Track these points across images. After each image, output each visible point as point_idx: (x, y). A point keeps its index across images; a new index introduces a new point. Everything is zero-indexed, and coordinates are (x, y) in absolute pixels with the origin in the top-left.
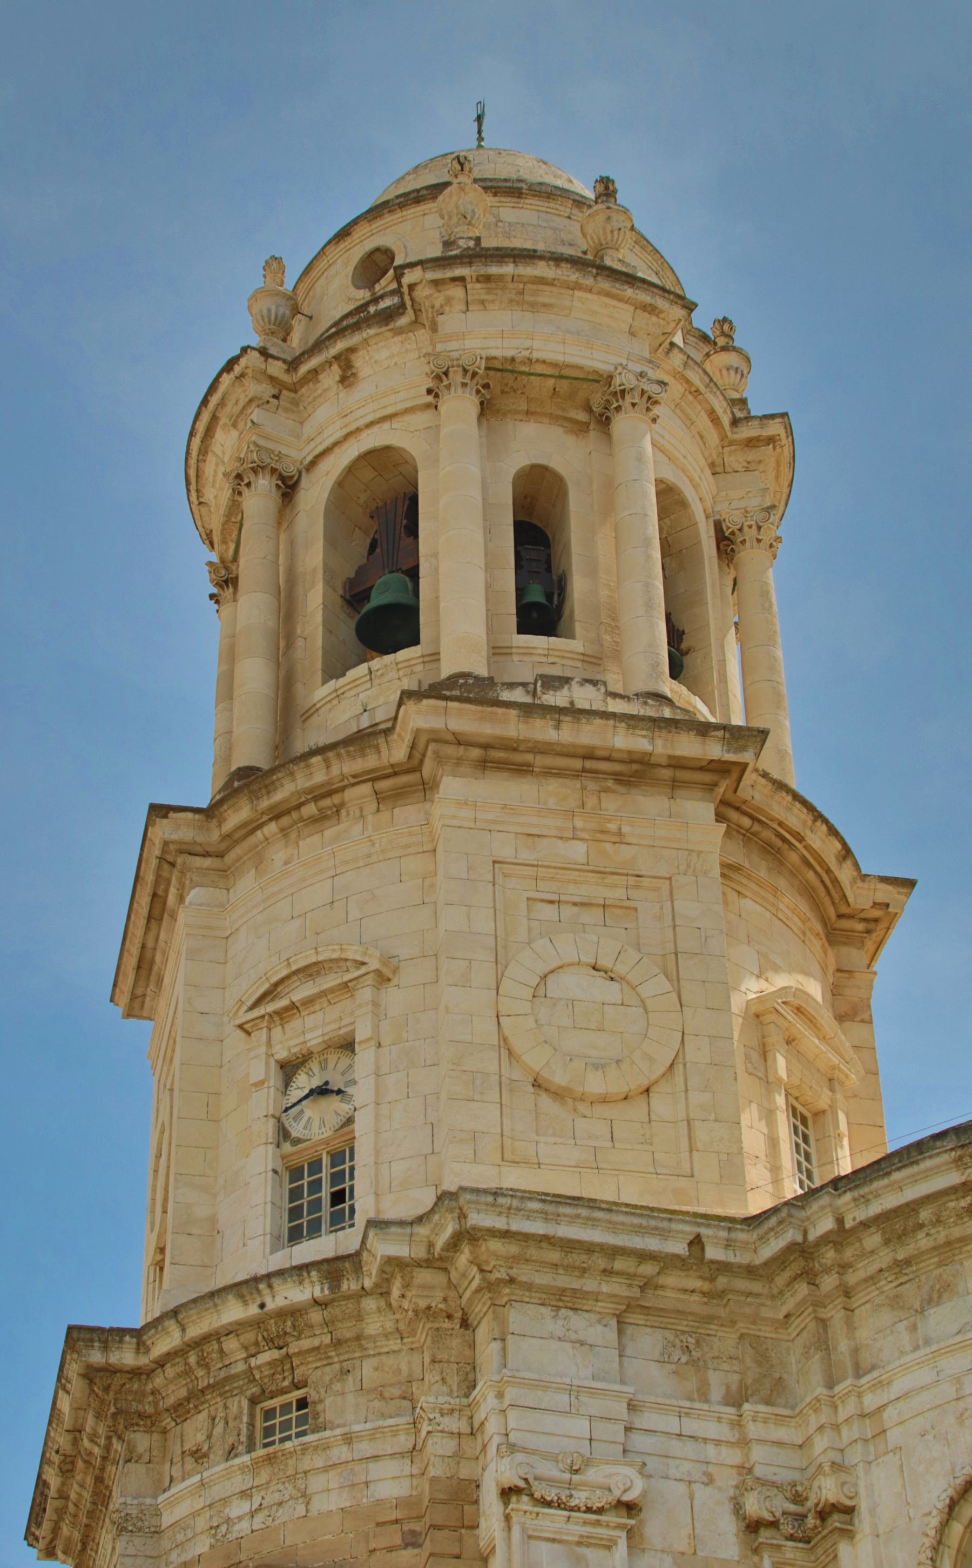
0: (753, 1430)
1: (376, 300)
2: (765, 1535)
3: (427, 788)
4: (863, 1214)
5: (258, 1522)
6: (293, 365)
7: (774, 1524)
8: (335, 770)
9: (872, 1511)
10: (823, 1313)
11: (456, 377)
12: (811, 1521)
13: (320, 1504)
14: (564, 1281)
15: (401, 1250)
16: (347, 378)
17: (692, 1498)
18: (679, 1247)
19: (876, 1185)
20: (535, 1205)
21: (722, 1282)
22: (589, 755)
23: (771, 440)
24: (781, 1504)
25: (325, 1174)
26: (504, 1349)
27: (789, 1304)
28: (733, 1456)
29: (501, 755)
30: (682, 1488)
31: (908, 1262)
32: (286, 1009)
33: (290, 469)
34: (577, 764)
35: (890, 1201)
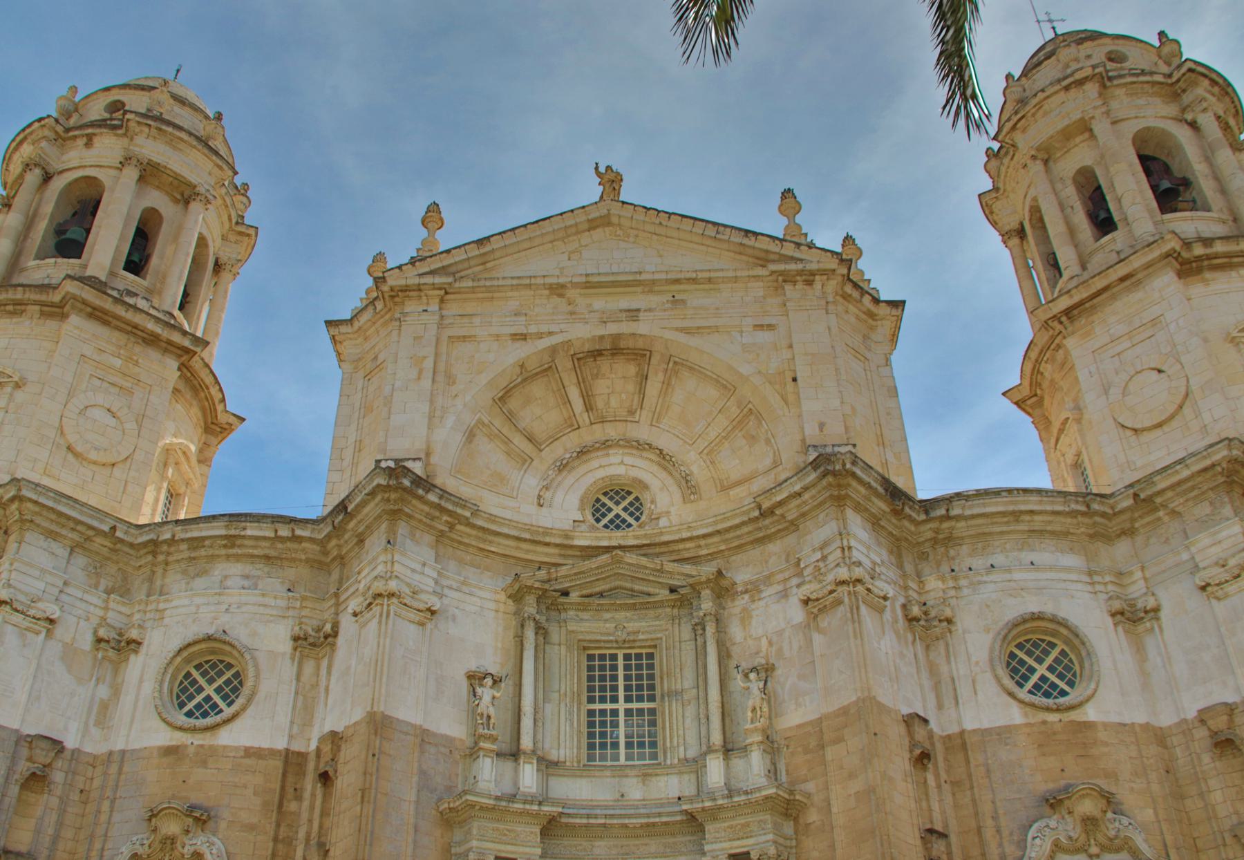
0: (112, 605)
1: (111, 119)
2: (103, 645)
3: (64, 317)
6: (68, 130)
7: (108, 642)
8: (27, 296)
10: (155, 569)
11: (134, 162)
14: (54, 527)
16: (89, 144)
17: (78, 624)
18: (106, 528)
20: (52, 494)
21: (119, 546)
22: (136, 327)
23: (249, 235)
24: (113, 635)
26: (19, 547)
27: (143, 562)
28: (101, 613)
29: (100, 314)
30: (75, 619)
31: (194, 558)
33: (51, 171)
34: (130, 329)
35: (196, 534)
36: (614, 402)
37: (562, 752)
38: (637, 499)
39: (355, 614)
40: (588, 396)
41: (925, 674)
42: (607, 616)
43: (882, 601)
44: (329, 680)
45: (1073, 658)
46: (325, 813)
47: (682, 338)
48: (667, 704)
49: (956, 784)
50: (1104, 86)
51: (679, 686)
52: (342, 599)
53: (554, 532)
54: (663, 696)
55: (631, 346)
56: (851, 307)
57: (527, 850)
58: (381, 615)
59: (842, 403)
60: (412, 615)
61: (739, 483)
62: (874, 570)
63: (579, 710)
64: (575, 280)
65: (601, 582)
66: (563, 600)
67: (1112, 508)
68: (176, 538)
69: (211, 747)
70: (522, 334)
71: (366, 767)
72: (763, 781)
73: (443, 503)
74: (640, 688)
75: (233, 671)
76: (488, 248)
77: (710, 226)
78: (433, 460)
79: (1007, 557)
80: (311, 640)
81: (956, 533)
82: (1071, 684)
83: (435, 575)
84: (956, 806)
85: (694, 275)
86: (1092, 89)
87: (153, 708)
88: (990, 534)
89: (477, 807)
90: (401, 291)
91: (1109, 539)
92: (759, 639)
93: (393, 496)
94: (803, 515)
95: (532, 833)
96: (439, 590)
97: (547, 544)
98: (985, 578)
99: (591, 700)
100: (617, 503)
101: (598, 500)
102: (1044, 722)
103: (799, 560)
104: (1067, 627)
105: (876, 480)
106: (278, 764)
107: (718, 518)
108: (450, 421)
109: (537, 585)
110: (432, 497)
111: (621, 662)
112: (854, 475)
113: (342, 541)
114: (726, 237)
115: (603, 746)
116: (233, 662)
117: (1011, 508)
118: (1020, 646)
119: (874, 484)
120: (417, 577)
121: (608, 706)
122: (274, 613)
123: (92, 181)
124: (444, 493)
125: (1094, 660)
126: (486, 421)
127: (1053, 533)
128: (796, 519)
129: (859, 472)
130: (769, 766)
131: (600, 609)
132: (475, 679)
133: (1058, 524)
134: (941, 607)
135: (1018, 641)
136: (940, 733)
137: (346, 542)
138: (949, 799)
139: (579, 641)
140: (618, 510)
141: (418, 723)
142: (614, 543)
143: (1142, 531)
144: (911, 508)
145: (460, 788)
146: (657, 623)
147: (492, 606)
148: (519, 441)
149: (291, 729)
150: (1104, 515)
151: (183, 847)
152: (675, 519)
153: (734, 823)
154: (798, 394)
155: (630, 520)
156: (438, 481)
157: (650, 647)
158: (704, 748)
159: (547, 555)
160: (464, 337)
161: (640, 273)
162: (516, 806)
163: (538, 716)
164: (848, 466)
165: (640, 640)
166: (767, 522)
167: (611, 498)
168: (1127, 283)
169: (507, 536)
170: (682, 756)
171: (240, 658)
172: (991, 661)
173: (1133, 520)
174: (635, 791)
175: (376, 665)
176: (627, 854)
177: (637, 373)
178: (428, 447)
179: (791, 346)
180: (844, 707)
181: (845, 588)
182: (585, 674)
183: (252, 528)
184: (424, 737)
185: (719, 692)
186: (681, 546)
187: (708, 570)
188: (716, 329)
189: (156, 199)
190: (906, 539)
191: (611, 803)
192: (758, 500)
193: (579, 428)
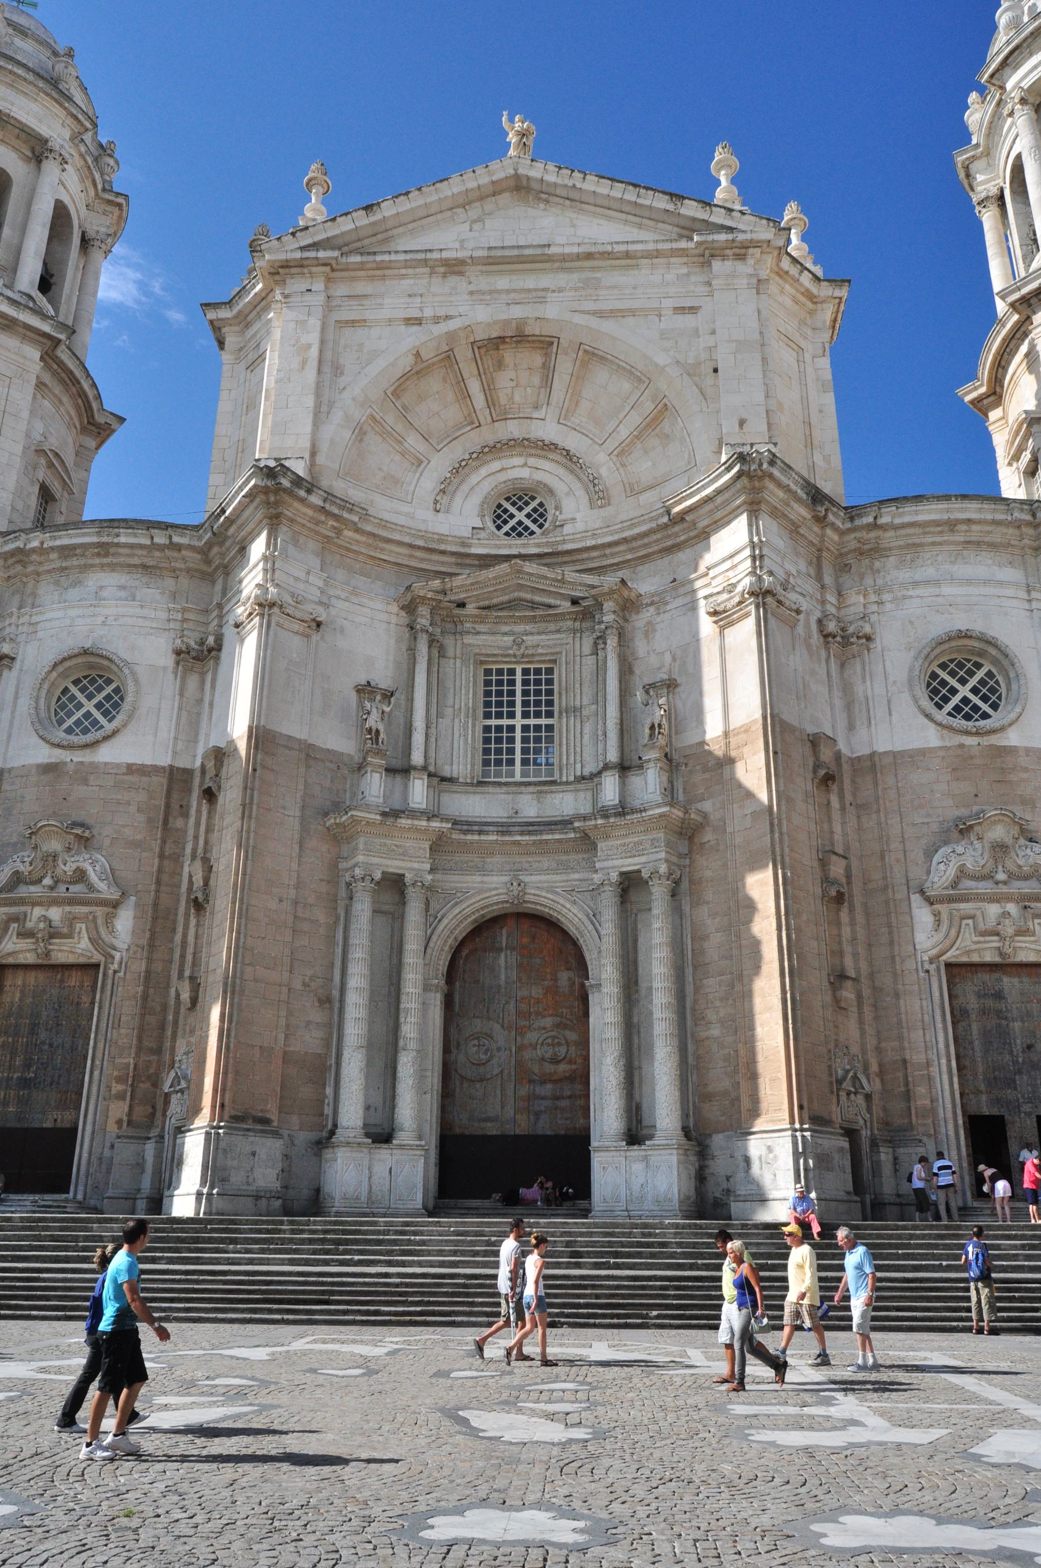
4: (51, 544)
9: (22, 661)
10: (25, 579)
23: (119, 205)
27: (12, 572)
36: (517, 398)
38: (541, 505)
41: (837, 693)
42: (506, 628)
47: (594, 322)
51: (578, 703)
54: (560, 713)
55: (537, 333)
56: (787, 287)
57: (416, 866)
58: (261, 626)
59: (767, 397)
60: (296, 626)
62: (787, 581)
63: (474, 726)
64: (477, 254)
66: (458, 611)
69: (91, 764)
72: (658, 798)
73: (327, 506)
74: (537, 703)
75: (113, 686)
78: (320, 459)
80: (193, 654)
81: (884, 544)
82: (995, 706)
83: (321, 584)
84: (860, 829)
85: (609, 248)
88: (921, 545)
90: (282, 267)
96: (325, 600)
97: (443, 552)
98: (910, 593)
99: (487, 715)
100: (520, 509)
101: (499, 506)
102: (961, 746)
104: (996, 646)
105: (796, 483)
106: (165, 781)
108: (337, 416)
110: (315, 499)
111: (519, 677)
112: (771, 476)
114: (647, 202)
115: (498, 763)
117: (945, 517)
118: (943, 666)
119: (793, 487)
120: (301, 586)
121: (505, 722)
122: (154, 625)
124: (329, 496)
129: (776, 472)
130: (666, 785)
131: (498, 621)
132: (366, 690)
133: (998, 535)
134: (861, 623)
140: (520, 516)
142: (514, 551)
144: (835, 514)
146: (558, 636)
147: (384, 617)
148: (413, 441)
149: (175, 745)
152: (580, 526)
153: (627, 841)
156: (325, 483)
158: (601, 765)
160: (353, 321)
161: (549, 246)
163: (433, 730)
164: (765, 466)
165: (542, 654)
166: (677, 529)
167: (514, 504)
169: (400, 543)
170: (579, 773)
172: (910, 680)
174: (530, 808)
177: (544, 364)
182: (481, 689)
183: (127, 535)
184: (309, 753)
186: (585, 555)
188: (632, 312)
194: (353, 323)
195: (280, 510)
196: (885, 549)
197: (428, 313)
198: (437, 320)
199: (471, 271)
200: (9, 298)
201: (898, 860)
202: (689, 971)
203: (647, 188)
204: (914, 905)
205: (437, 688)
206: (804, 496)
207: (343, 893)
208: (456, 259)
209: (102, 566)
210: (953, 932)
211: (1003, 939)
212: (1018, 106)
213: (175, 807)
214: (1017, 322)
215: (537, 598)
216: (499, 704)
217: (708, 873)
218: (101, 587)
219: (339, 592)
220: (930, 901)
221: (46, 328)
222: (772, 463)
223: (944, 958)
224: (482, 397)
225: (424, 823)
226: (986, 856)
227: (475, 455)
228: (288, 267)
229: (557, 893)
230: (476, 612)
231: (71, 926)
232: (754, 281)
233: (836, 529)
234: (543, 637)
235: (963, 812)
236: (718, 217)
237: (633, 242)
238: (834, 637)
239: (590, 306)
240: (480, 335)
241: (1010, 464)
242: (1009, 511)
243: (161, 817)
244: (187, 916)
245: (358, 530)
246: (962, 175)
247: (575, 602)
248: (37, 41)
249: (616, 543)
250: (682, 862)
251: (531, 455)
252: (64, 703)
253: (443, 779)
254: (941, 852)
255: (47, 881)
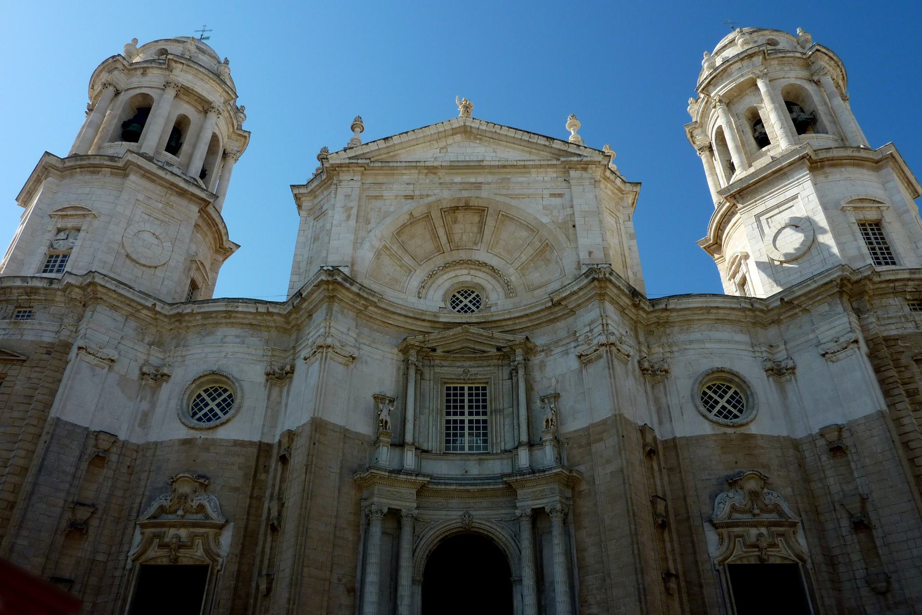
0: (152, 352)
1: (159, 59)
3: (126, 176)
4: (198, 311)
5: (5, 337)
7: (149, 375)
10: (180, 331)
12: (159, 376)
13: (25, 338)
15: (73, 282)
16: (144, 74)
18: (149, 304)
19: (204, 305)
23: (245, 137)
25: (59, 260)
26: (93, 315)
27: (173, 326)
28: (145, 357)
29: (149, 175)
31: (205, 325)
32: (65, 215)
34: (168, 185)
35: (206, 310)
36: (464, 238)
37: (430, 444)
39: (305, 359)
40: (449, 233)
41: (652, 403)
42: (459, 364)
43: (626, 357)
44: (288, 399)
45: (742, 396)
46: (282, 481)
47: (507, 200)
48: (494, 417)
49: (670, 470)
50: (765, 58)
51: (501, 407)
52: (298, 350)
53: (428, 313)
54: (491, 413)
56: (609, 185)
57: (408, 504)
58: (322, 358)
60: (341, 359)
61: (539, 287)
63: (441, 419)
64: (444, 164)
65: (455, 344)
67: (767, 307)
68: (194, 312)
70: (410, 196)
71: (309, 451)
73: (361, 293)
74: (477, 407)
75: (228, 393)
76: (390, 143)
77: (526, 133)
79: (702, 334)
80: (277, 375)
81: (671, 319)
82: (741, 411)
83: (355, 336)
86: (758, 59)
87: (176, 414)
89: (378, 477)
90: (338, 167)
91: (765, 326)
92: (550, 379)
93: (331, 287)
94: (579, 305)
95: (411, 493)
97: (424, 320)
98: (688, 347)
99: (448, 414)
100: (466, 298)
101: (454, 296)
102: (725, 434)
103: (576, 332)
104: (738, 377)
105: (624, 285)
106: (254, 450)
107: (527, 307)
108: (367, 245)
109: (417, 344)
110: (355, 289)
111: (466, 392)
112: (610, 281)
113: (298, 316)
114: (535, 141)
116: (227, 388)
117: (705, 305)
118: (709, 388)
121: (459, 418)
122: (255, 358)
123: (145, 96)
124: (362, 287)
125: (755, 397)
126: (388, 247)
127: (731, 321)
128: (574, 308)
129: (613, 279)
133: (734, 315)
135: (708, 385)
136: (660, 439)
137: (301, 316)
138: (666, 478)
139: (441, 378)
140: (466, 302)
141: (342, 425)
142: (464, 321)
143: (784, 321)
144: (644, 303)
145: (367, 466)
146: (489, 368)
147: (389, 355)
148: (407, 259)
149: (263, 429)
150: (762, 311)
151: (192, 501)
152: (500, 307)
154: (575, 235)
155: (473, 308)
157: (484, 383)
158: (516, 443)
159: (424, 327)
160: (376, 196)
161: (483, 161)
162: (401, 476)
163: (417, 422)
164: (607, 275)
166: (557, 309)
167: (462, 295)
168: (778, 174)
169: (400, 315)
170: (503, 448)
171: (233, 385)
172: (692, 396)
173: (780, 315)
174: (474, 469)
175: (318, 389)
176: (469, 508)
178: (353, 260)
179: (572, 207)
180: (604, 420)
181: (604, 348)
182: (445, 398)
183: (243, 307)
184: (345, 434)
185: (526, 410)
186: (504, 323)
187: (520, 338)
188: (528, 196)
189: (187, 109)
190: (641, 322)
191: (459, 476)
192: (551, 295)
193: (444, 252)
194: (376, 197)
195: (335, 293)
196: (672, 322)
197: (417, 193)
198: (421, 197)
199: (441, 173)
200: (185, 179)
201: (694, 502)
202: (576, 571)
203: (534, 134)
204: (706, 529)
205: (420, 396)
206: (628, 293)
207: (363, 521)
208: (433, 166)
209: (227, 323)
210: (732, 546)
211: (760, 550)
212: (719, 104)
213: (261, 466)
214: (728, 207)
215: (477, 347)
216: (455, 407)
217: (585, 509)
218: (225, 336)
219: (365, 341)
220: (715, 526)
221: (203, 195)
222: (611, 274)
223: (727, 561)
224: (446, 237)
225: (414, 478)
226: (747, 498)
227: (441, 268)
228: (341, 167)
229: (492, 522)
230: (442, 354)
231: (192, 541)
232: (592, 181)
233: (645, 311)
234: (480, 369)
235: (730, 472)
236: (572, 149)
237: (528, 160)
238: (647, 371)
239: (505, 192)
240: (446, 205)
241: (730, 280)
242: (740, 303)
243: (252, 473)
244: (266, 535)
245: (376, 307)
246: (689, 136)
247: (499, 349)
248: (210, 56)
249: (522, 317)
250: (568, 502)
251: (472, 269)
252: (199, 403)
253: (424, 451)
254: (718, 497)
255: (180, 512)
